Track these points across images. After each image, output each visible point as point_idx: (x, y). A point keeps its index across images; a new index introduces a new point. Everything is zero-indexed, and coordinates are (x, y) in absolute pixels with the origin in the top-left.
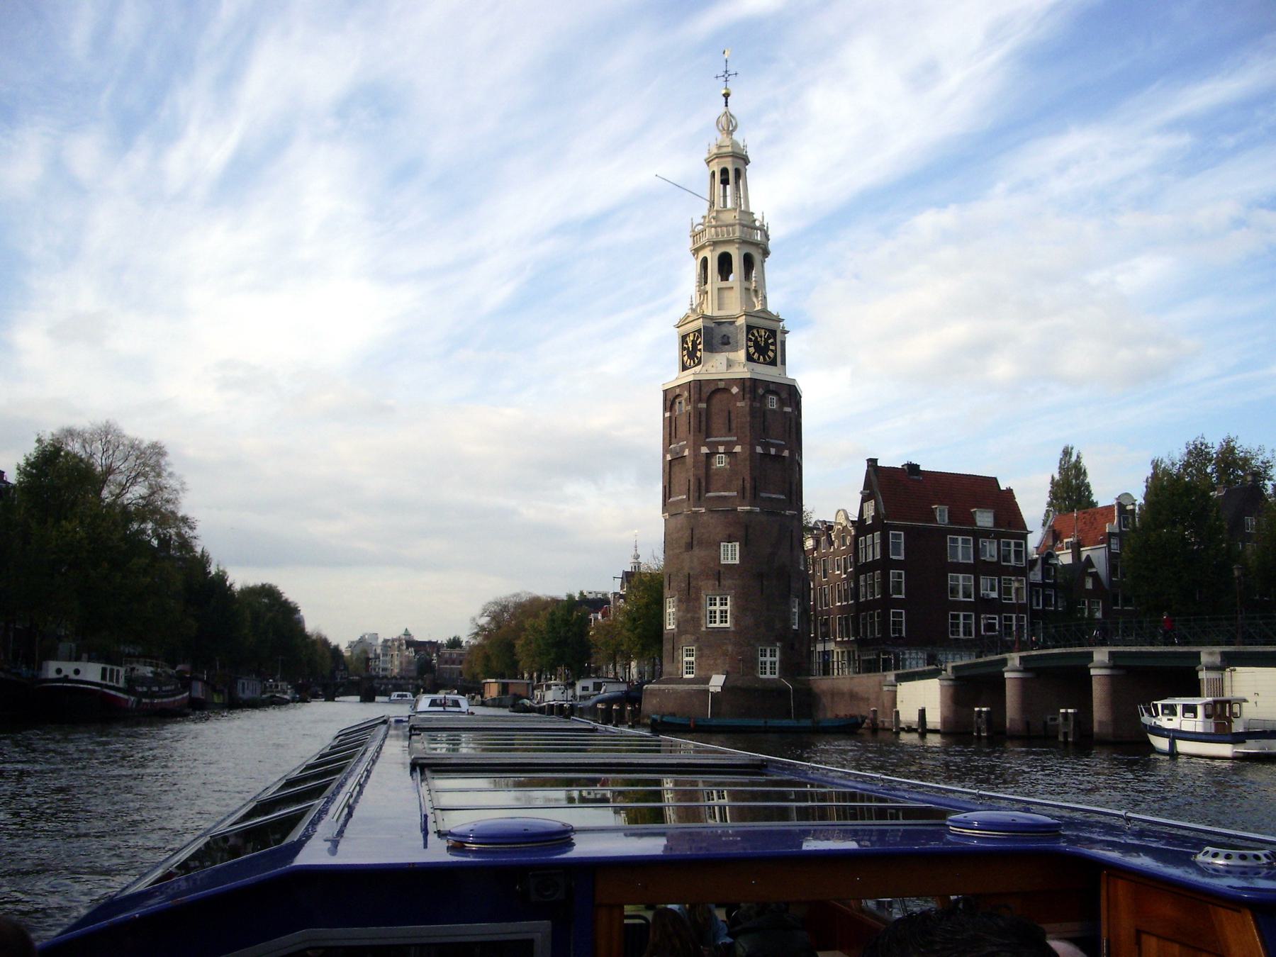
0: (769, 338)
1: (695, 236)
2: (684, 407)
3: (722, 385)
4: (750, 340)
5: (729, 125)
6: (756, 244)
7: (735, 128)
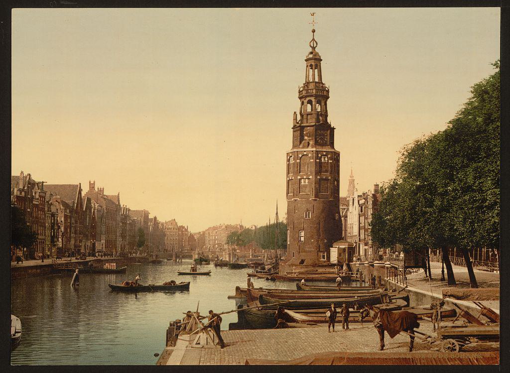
1: (299, 92)
2: (292, 161)
3: (305, 153)
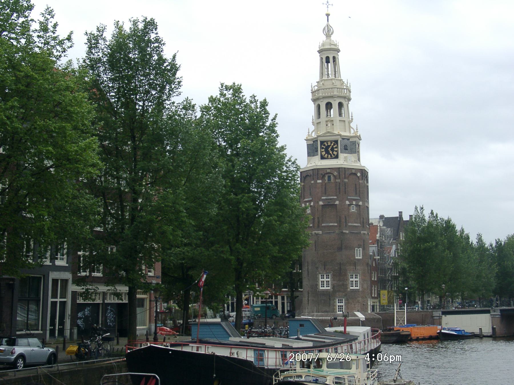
0: (334, 145)
4: (323, 148)
5: (328, 32)
6: (332, 97)
7: (332, 34)
